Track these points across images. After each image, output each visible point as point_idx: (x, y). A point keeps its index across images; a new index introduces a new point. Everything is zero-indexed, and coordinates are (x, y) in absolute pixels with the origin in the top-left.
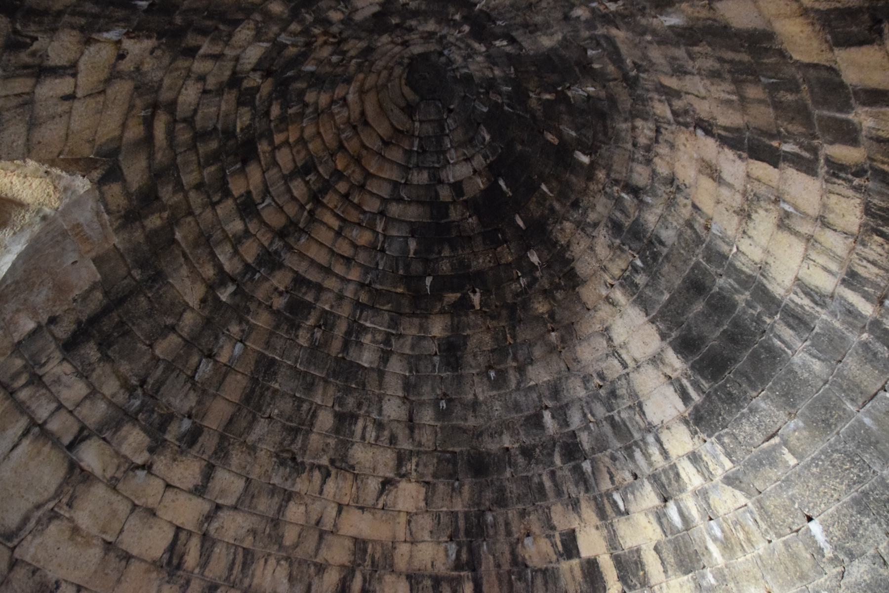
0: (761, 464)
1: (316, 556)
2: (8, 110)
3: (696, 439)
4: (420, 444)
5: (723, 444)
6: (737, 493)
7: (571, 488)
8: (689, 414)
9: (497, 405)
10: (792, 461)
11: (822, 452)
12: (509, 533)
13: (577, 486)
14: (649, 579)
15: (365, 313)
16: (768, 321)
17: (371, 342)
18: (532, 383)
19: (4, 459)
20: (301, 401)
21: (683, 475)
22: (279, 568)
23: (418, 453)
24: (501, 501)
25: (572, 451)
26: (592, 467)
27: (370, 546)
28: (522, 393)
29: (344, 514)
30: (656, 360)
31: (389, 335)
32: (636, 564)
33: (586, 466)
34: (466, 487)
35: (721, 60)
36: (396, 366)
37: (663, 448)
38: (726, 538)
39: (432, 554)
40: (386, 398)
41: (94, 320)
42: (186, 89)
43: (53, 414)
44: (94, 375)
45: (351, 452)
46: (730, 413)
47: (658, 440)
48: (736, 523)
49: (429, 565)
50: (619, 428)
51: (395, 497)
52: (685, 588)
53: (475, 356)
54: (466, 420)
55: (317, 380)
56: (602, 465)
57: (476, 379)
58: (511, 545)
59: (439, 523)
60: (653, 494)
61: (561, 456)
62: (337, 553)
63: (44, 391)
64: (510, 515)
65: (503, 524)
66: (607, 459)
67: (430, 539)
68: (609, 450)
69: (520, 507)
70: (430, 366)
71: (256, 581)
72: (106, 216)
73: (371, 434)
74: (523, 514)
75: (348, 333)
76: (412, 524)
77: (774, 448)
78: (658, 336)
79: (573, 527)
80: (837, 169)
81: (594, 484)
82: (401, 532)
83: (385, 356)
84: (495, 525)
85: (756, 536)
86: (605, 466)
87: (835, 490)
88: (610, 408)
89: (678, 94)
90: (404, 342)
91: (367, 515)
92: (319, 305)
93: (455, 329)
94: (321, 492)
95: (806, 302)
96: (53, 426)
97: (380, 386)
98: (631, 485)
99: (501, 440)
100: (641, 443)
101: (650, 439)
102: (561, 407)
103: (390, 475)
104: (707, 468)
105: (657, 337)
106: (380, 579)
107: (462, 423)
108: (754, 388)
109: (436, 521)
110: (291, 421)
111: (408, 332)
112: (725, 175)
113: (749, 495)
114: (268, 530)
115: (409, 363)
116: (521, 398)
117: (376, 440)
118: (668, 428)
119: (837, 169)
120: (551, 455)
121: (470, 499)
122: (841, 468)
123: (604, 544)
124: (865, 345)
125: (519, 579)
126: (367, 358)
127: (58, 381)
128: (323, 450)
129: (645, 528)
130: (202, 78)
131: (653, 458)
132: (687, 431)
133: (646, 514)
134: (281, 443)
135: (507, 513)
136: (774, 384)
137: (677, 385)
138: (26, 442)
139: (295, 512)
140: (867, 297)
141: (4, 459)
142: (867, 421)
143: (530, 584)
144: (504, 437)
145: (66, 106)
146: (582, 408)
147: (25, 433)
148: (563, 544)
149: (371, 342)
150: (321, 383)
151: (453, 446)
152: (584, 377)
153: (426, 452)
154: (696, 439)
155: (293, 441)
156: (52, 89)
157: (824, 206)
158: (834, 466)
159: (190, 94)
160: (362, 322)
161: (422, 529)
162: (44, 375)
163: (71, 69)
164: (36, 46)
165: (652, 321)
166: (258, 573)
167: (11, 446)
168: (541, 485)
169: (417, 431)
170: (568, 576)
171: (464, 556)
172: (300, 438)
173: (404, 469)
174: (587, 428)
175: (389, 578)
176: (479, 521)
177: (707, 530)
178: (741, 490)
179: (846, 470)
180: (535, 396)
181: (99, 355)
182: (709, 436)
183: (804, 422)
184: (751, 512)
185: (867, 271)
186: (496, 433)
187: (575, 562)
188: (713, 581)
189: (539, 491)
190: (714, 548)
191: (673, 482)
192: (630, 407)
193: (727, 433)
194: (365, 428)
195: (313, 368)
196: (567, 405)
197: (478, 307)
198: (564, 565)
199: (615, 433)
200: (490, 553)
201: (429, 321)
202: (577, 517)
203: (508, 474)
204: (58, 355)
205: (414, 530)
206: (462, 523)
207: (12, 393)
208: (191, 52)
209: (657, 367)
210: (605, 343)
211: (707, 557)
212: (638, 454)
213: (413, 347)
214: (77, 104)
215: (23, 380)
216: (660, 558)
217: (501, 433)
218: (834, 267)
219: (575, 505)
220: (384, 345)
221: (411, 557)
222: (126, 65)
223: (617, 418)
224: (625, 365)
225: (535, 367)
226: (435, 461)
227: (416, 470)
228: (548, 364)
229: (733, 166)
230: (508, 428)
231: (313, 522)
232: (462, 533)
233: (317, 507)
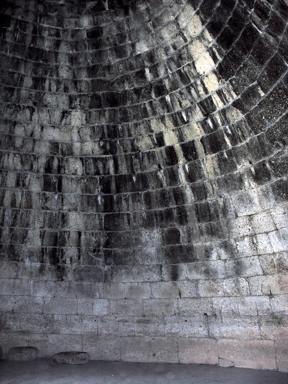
1: (33, 151)
3: (220, 82)
4: (81, 91)
5: (232, 84)
6: (239, 111)
7: (160, 111)
8: (217, 68)
9: (121, 67)
10: (262, 94)
11: (275, 89)
12: (130, 135)
13: (163, 109)
14: (198, 156)
15: (42, 19)
17: (49, 35)
18: (139, 53)
20: (14, 73)
21: (214, 102)
22: (15, 158)
23: (80, 96)
24: (125, 119)
25: (160, 90)
26: (171, 98)
27: (60, 145)
28: (134, 59)
29: (44, 130)
30: (201, 37)
31: (57, 30)
32: (192, 148)
33: (168, 98)
34: (107, 113)
36: (64, 49)
37: (205, 87)
38: (233, 135)
39: (91, 147)
40: (60, 67)
45: (45, 97)
46: (236, 68)
47: (202, 83)
48: (238, 127)
49: (91, 152)
50: (184, 77)
51: (70, 120)
52: (214, 160)
53: (108, 39)
54: (105, 76)
55: (20, 61)
56: (175, 97)
57: (109, 52)
58: (131, 141)
59: (94, 131)
60: (200, 112)
61: (155, 93)
62: (43, 149)
64: (130, 125)
65: (127, 130)
66: (178, 94)
67: (90, 140)
68: (179, 89)
69: (135, 121)
70: (83, 47)
71: (5, 164)
73: (54, 88)
74: (136, 125)
75: (34, 32)
76: (81, 132)
77: (254, 87)
78: (200, 22)
79: (162, 130)
81: (172, 108)
82: (76, 137)
83: (57, 44)
84: (123, 131)
86: (177, 98)
87: (279, 109)
88: (179, 66)
90: (67, 34)
91: (57, 130)
92: (14, 17)
93: (95, 23)
94: (31, 120)
97: (56, 61)
98: (190, 108)
99: (124, 86)
100: (194, 85)
101: (199, 82)
102: (154, 66)
103: (66, 108)
104: (225, 98)
105: (200, 23)
106: (67, 161)
107: (102, 78)
109: (93, 131)
110: (10, 84)
111: (69, 27)
113: (244, 112)
114: (7, 141)
115: (72, 46)
116: (134, 62)
117: (57, 91)
118: (207, 76)
120: (150, 93)
121: (109, 118)
122: (282, 98)
123: (177, 139)
125: (136, 157)
126: (47, 45)
128: (29, 98)
129: (197, 130)
131: (200, 93)
132: (216, 77)
133: (197, 123)
134: (6, 96)
135: (128, 125)
136: (254, 50)
137: (210, 51)
139: (19, 131)
143: (141, 159)
144: (125, 84)
146: (165, 66)
148: (157, 139)
149: (49, 35)
150: (23, 62)
151: (99, 91)
152: (166, 48)
153: (84, 95)
154: (220, 82)
155: (12, 95)
158: (279, 97)
160: (41, 24)
161: (86, 135)
165: (198, 13)
166: (6, 161)
168: (145, 109)
169: (78, 84)
170: (160, 155)
171: (108, 147)
172: (15, 93)
173: (73, 105)
174: (168, 77)
175: (71, 160)
176: (114, 129)
177: (224, 130)
178: (240, 110)
179: (285, 98)
180: (140, 60)
182: (226, 80)
183: (267, 72)
184: (245, 121)
186: (122, 81)
187: (163, 148)
188: (226, 156)
189: (144, 112)
190: (227, 139)
191: (210, 106)
192: (189, 65)
193: (234, 79)
194: (50, 84)
195: (17, 54)
196: (157, 64)
197: (107, 9)
198: (158, 150)
199: (181, 79)
200: (121, 145)
201: (80, 19)
202: (163, 125)
203: (128, 105)
205: (82, 135)
206: (106, 131)
209: (201, 41)
210: (176, 27)
211: (224, 144)
212: (193, 91)
213: (73, 36)
216: (203, 145)
217: (123, 82)
219: (163, 119)
220: (56, 37)
221: (81, 149)
223: (182, 71)
224: (185, 40)
225: (140, 43)
226: (90, 99)
227: (80, 105)
228: (147, 41)
230: (127, 79)
231: (29, 135)
232: (106, 136)
233: (30, 127)
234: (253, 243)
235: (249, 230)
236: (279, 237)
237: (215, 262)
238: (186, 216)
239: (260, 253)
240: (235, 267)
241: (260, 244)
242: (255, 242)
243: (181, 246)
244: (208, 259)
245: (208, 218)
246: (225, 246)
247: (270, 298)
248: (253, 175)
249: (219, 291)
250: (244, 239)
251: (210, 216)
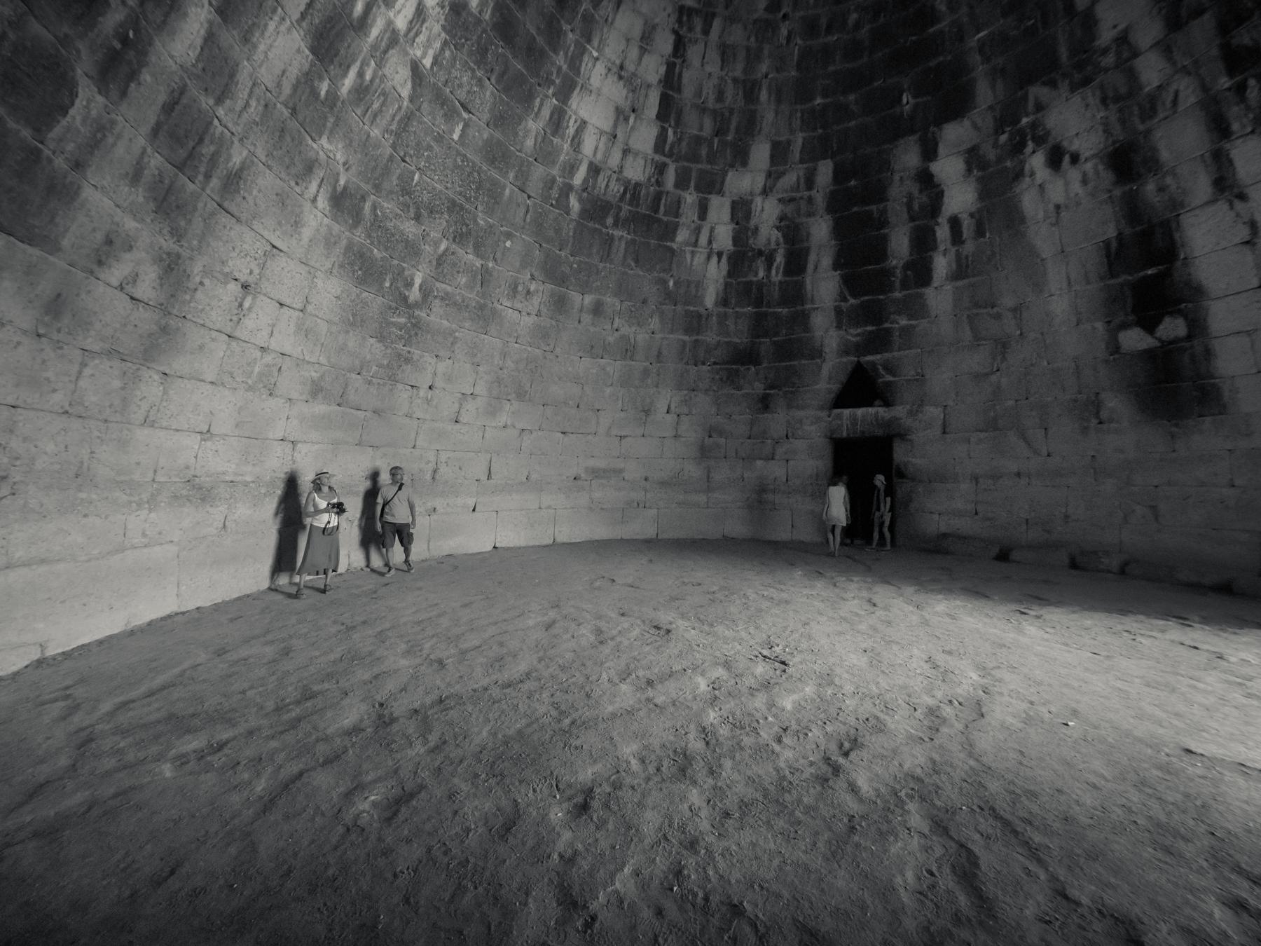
0: (443, 104)
5: (442, 50)
10: (456, 137)
11: (473, 163)
16: (550, 91)
35: (731, 111)
38: (367, 89)
80: (661, 169)
85: (383, 122)
89: (706, 32)
95: (571, 131)
104: (417, 35)
108: (498, 81)
112: (646, 58)
119: (661, 169)
124: (553, 181)
140: (585, 180)
142: (507, 191)
157: (636, 154)
178: (413, 88)
185: (602, 181)
218: (599, 156)
229: (652, 69)
234: (241, 305)
235: (251, 272)
236: (299, 328)
237: (109, 290)
238: (133, 75)
239: (237, 334)
240: (150, 335)
241: (253, 315)
242: (246, 304)
243: (39, 151)
244: (95, 267)
245: (182, 153)
246: (169, 266)
247: (202, 440)
248: (335, 188)
249: (54, 391)
250: (226, 283)
251: (191, 156)
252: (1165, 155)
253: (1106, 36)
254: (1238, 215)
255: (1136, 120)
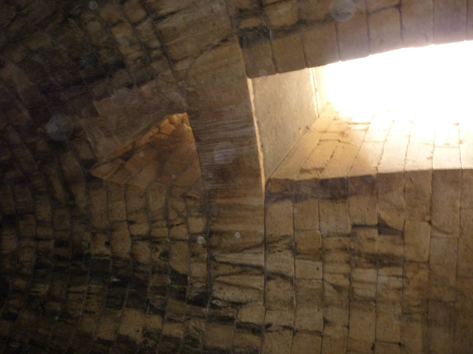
2: (161, 219)
19: (181, 10)
41: (101, 77)
42: (49, 215)
43: (139, 22)
44: (105, 39)
63: (142, 40)
72: (89, 139)
96: (141, 13)
127: (132, 44)
130: (40, 223)
138: (163, 12)
141: (181, 10)
145: (132, 218)
147: (162, 18)
156: (141, 229)
159: (44, 212)
162: (139, 50)
163: (135, 239)
164: (158, 254)
167: (174, 16)
181: (100, 52)
204: (129, 62)
207: (162, 47)
208: (60, 243)
214: (125, 218)
215: (155, 53)
222: (103, 238)
252: (223, 346)
253: (139, 338)
254: (277, 331)
255: (194, 349)
